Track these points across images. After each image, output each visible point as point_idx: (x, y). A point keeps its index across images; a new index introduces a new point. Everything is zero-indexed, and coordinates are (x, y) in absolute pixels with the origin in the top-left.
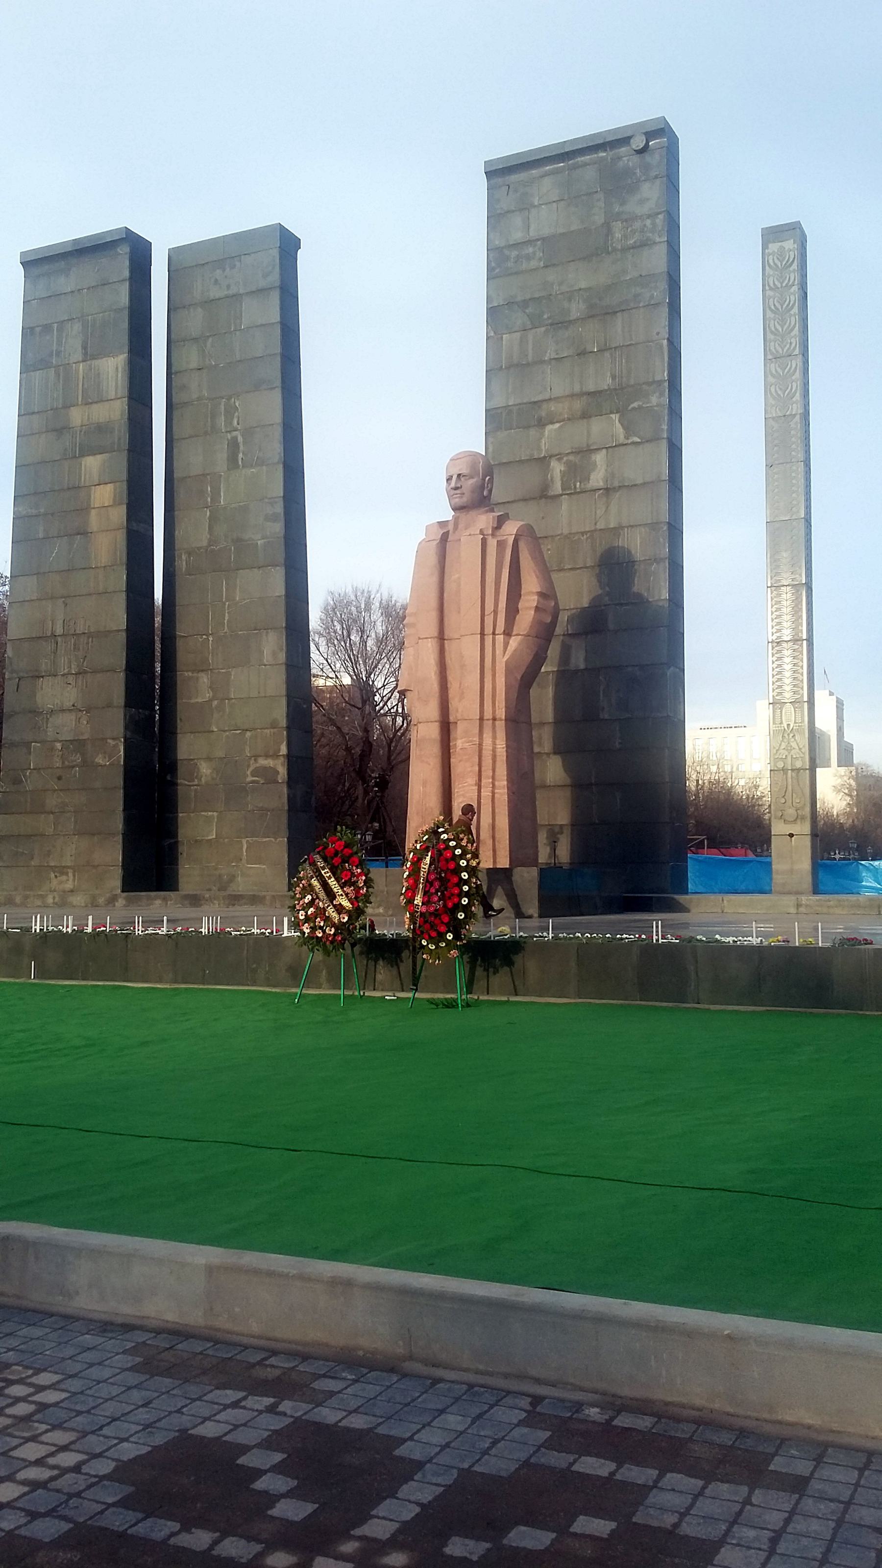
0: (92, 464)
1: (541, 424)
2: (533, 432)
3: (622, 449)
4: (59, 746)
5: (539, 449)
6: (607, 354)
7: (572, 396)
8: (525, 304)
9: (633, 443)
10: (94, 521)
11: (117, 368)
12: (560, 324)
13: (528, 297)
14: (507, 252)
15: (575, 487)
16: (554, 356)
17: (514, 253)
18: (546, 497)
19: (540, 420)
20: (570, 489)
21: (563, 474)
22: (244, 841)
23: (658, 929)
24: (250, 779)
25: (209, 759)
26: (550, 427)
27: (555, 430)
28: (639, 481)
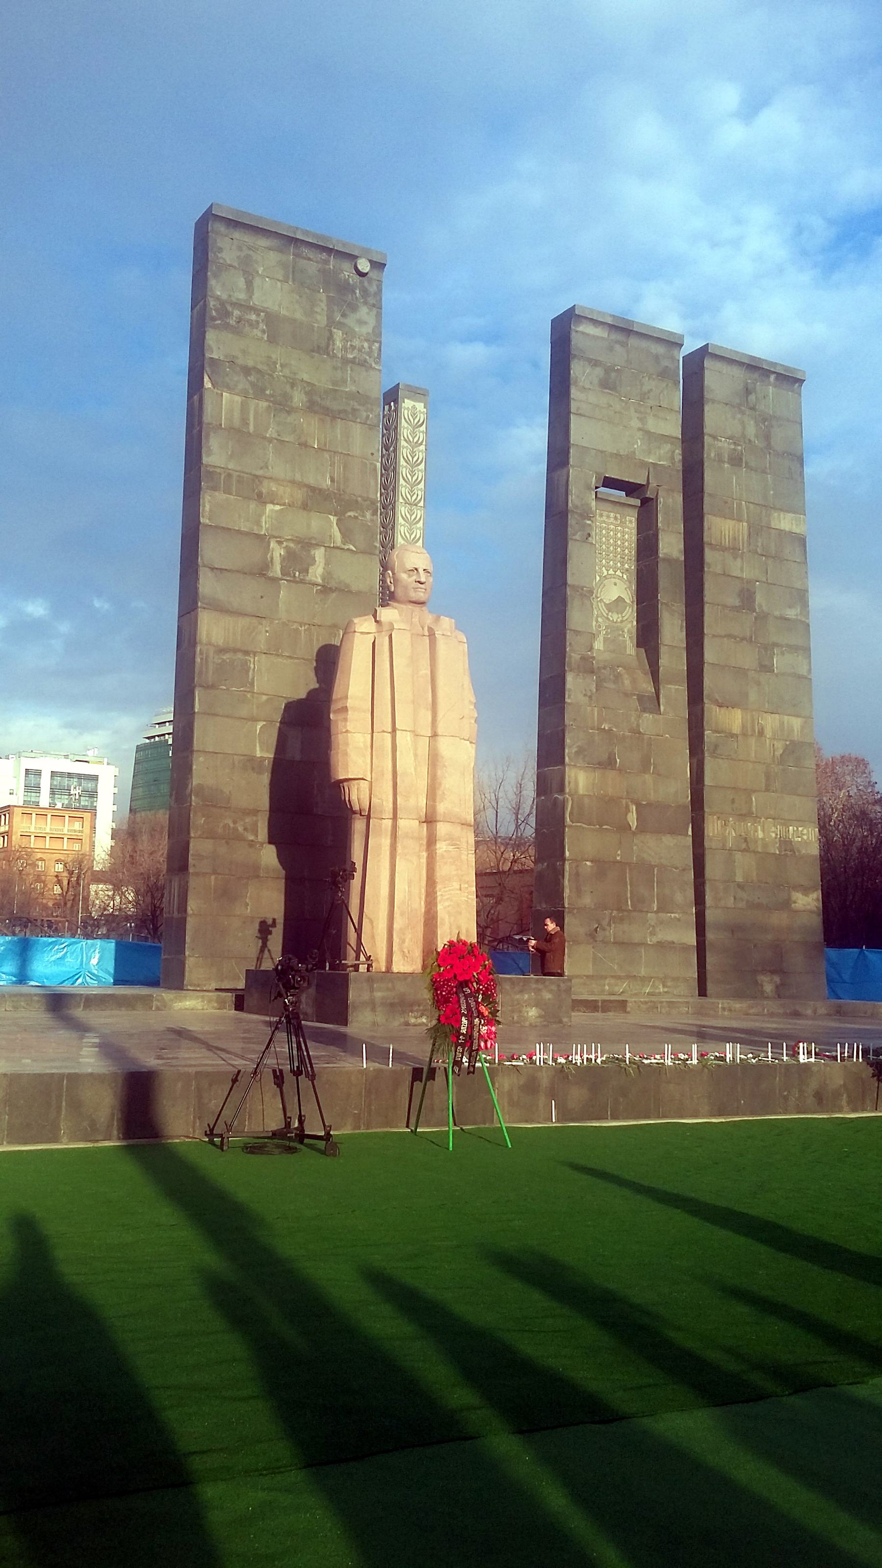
1: (262, 499)
2: (253, 505)
3: (338, 551)
5: (258, 523)
6: (327, 455)
7: (293, 482)
8: (247, 371)
9: (348, 549)
12: (282, 405)
13: (250, 363)
14: (229, 308)
15: (294, 576)
16: (275, 435)
17: (237, 313)
18: (262, 574)
19: (260, 495)
20: (289, 575)
21: (283, 559)
23: (342, 1029)
26: (269, 507)
27: (277, 511)
28: (354, 588)
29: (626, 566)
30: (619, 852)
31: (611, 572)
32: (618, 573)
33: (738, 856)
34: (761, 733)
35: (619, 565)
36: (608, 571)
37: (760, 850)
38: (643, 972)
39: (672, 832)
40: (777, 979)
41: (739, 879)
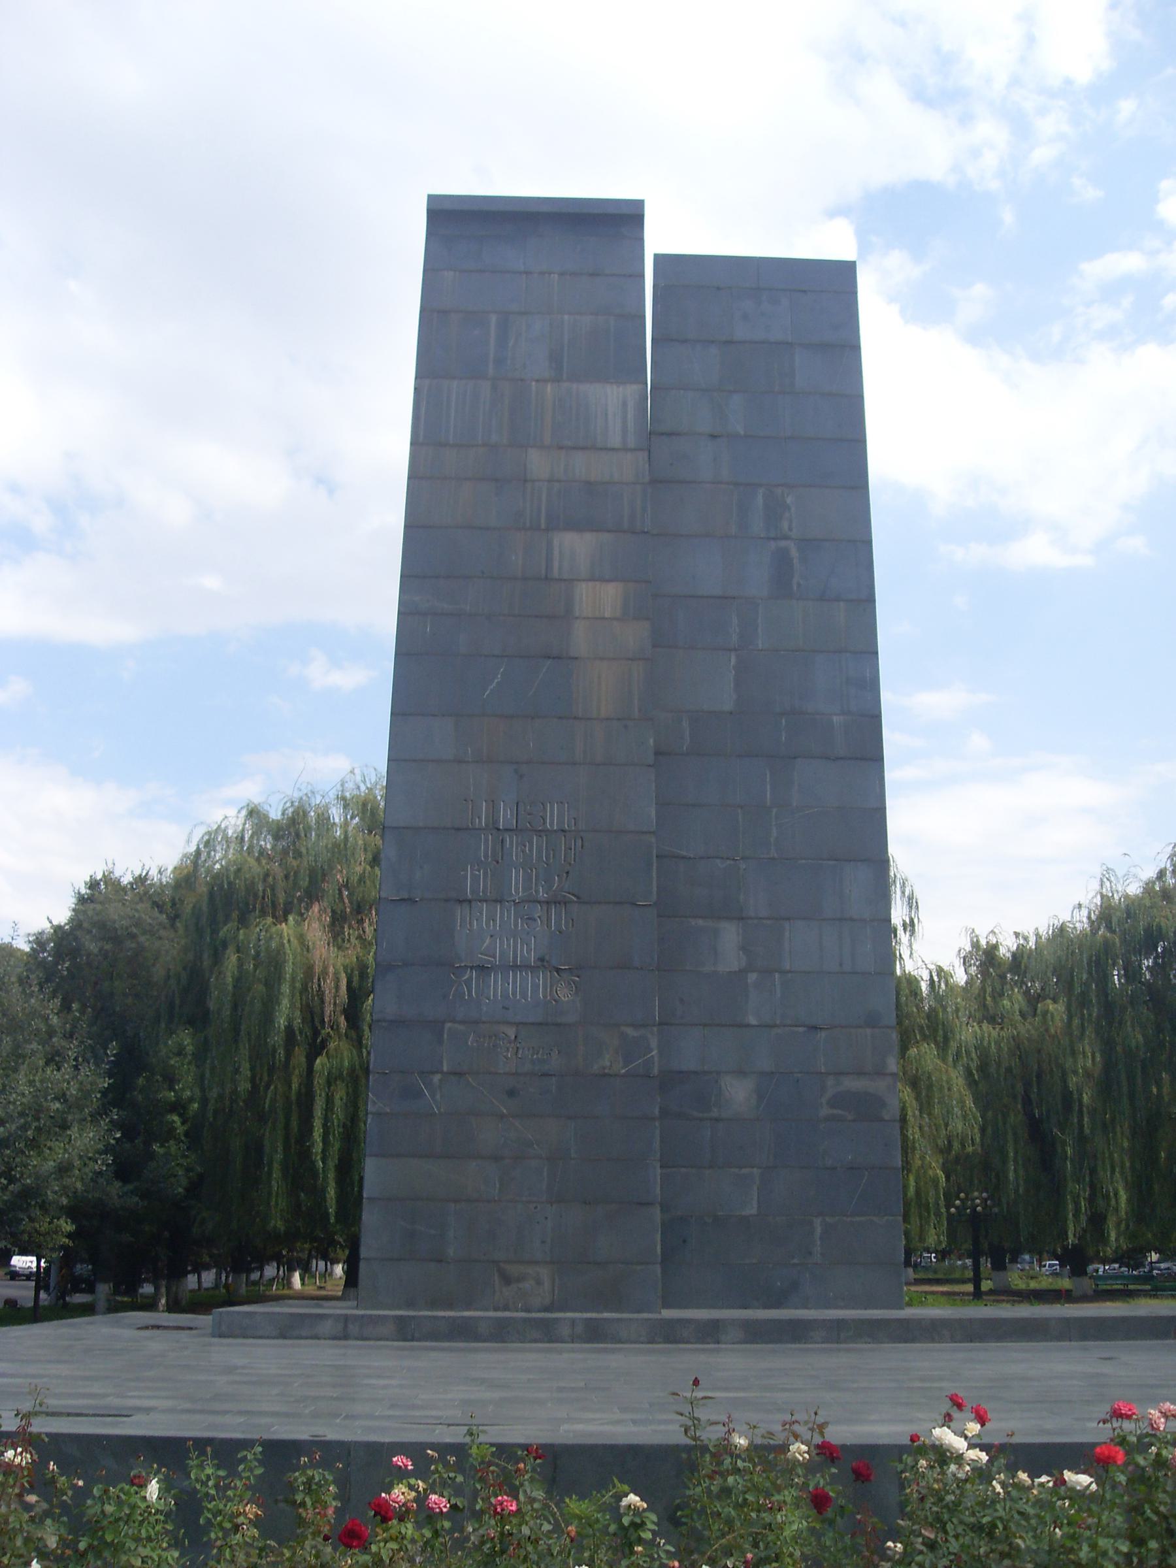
0: (575, 548)
4: (511, 1032)
10: (581, 639)
11: (625, 404)
22: (818, 1222)
24: (825, 1111)
25: (741, 1073)
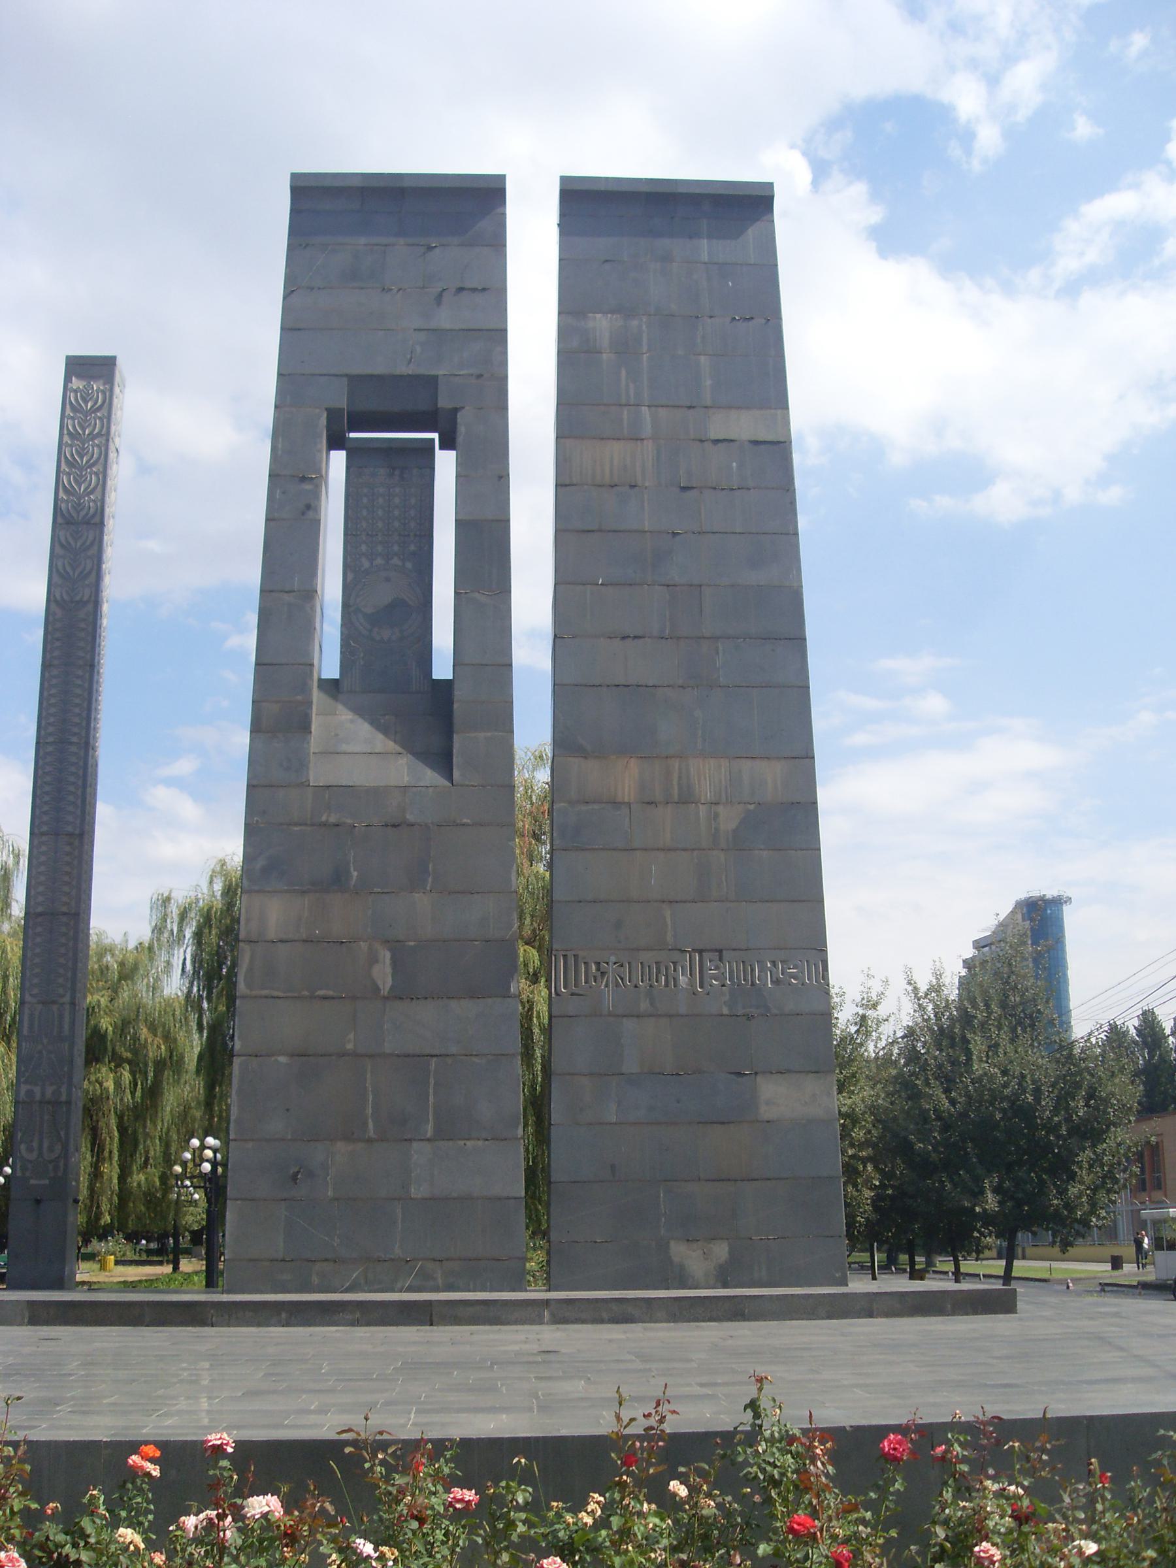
29: (412, 548)
30: (351, 1036)
31: (379, 561)
32: (396, 561)
33: (629, 1024)
34: (687, 798)
35: (396, 548)
36: (371, 561)
37: (683, 1010)
38: (398, 1252)
39: (473, 994)
40: (721, 1251)
41: (631, 1066)
